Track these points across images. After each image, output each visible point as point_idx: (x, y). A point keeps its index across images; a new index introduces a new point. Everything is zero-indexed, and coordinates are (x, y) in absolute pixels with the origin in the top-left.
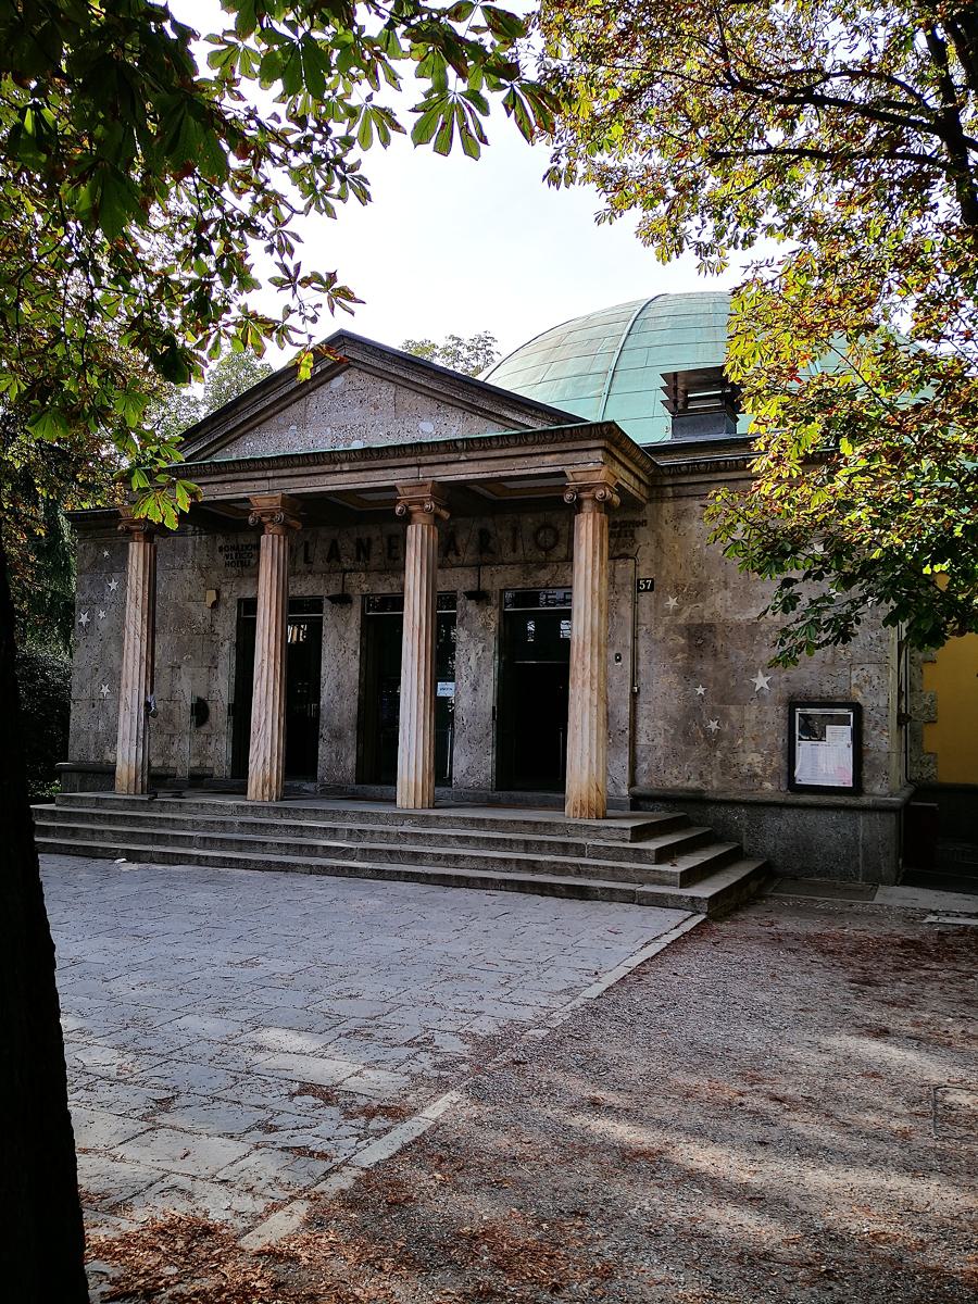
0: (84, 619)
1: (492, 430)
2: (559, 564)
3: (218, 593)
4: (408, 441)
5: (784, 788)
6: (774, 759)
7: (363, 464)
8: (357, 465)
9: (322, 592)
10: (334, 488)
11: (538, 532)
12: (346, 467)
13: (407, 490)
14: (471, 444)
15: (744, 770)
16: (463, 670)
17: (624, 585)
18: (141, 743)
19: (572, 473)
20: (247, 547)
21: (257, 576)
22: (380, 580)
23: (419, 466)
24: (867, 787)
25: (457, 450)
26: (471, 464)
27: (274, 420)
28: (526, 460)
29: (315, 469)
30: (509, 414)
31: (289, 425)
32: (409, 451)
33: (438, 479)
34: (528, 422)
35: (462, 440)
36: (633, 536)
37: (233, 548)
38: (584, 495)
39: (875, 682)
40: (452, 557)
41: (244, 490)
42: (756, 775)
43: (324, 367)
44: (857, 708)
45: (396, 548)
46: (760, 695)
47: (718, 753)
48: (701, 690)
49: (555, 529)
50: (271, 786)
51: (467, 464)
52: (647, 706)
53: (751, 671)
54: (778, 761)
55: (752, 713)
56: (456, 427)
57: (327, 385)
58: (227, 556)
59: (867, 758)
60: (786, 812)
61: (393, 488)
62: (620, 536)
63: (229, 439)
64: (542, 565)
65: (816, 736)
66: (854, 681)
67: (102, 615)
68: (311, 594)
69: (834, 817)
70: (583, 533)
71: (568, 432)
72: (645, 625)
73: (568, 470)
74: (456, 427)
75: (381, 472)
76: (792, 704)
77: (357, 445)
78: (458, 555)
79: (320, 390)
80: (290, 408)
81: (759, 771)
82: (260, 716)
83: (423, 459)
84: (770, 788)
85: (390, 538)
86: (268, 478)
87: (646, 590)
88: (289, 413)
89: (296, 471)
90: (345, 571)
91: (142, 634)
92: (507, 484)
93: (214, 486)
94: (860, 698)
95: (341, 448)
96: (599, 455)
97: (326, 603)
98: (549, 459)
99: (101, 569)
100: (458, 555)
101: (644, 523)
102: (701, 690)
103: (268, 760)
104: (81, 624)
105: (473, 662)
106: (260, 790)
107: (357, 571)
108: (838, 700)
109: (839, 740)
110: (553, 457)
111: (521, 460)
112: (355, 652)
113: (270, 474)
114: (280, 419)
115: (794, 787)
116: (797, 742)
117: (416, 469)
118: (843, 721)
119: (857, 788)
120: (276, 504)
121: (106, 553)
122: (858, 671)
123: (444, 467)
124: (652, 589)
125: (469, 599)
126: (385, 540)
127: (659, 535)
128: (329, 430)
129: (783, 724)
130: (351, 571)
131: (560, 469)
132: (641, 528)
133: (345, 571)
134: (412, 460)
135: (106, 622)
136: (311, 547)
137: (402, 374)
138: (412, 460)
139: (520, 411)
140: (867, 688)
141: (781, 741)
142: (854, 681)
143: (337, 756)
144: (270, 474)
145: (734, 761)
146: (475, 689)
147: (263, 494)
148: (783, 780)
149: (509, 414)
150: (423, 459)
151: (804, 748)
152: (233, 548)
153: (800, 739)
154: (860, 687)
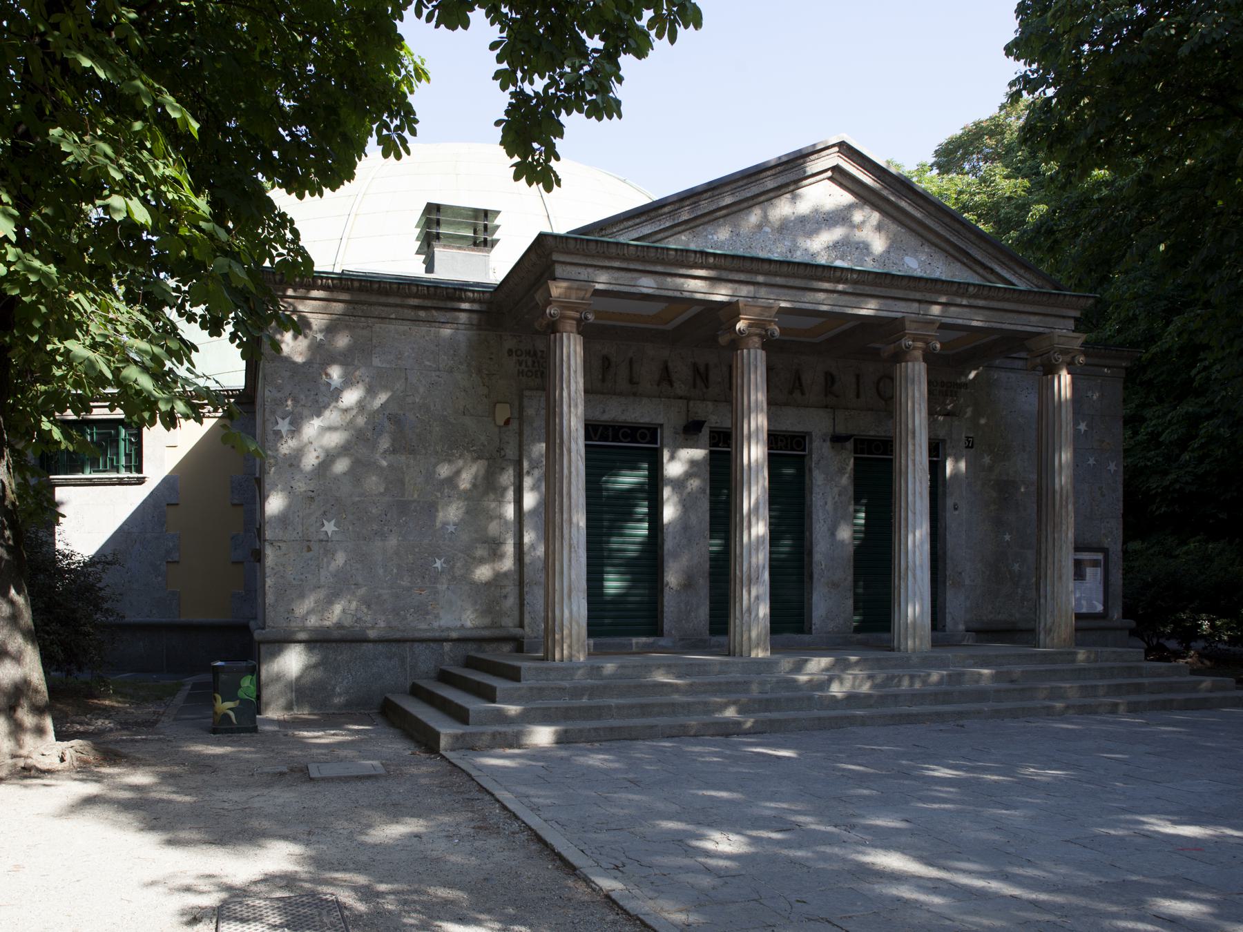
28: (1015, 316)
34: (1014, 279)
37: (528, 353)
47: (1020, 591)
48: (1007, 537)
58: (520, 364)
78: (803, 394)
89: (791, 282)
100: (803, 394)
102: (1007, 537)
105: (829, 507)
111: (1011, 315)
113: (760, 279)
117: (916, 305)
138: (918, 296)
152: (528, 353)
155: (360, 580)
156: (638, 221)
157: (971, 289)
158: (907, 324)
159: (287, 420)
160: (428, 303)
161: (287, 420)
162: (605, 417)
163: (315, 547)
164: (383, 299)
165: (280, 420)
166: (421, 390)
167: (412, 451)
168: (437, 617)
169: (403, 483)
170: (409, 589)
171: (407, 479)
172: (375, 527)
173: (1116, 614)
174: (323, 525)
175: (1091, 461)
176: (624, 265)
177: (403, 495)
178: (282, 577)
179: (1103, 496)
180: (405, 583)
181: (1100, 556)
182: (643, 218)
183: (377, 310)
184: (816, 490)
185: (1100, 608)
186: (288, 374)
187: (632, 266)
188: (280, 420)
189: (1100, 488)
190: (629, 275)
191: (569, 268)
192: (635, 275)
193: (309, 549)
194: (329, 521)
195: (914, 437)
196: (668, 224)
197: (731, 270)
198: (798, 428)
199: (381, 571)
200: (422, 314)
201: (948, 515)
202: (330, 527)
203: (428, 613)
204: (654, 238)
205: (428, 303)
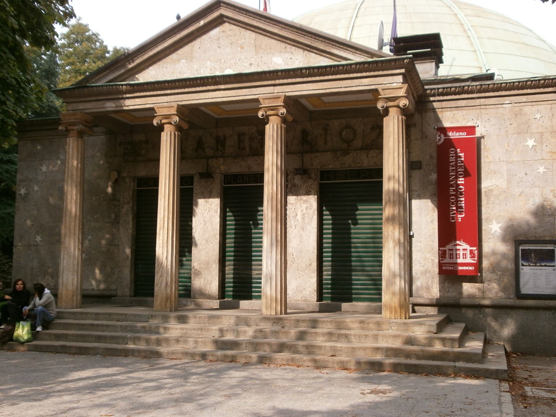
0: (23, 191)
2: (358, 152)
3: (119, 173)
4: (266, 69)
5: (512, 296)
6: (506, 277)
9: (191, 172)
10: (214, 100)
11: (342, 131)
13: (267, 101)
16: (293, 222)
18: (75, 274)
19: (383, 89)
21: (158, 160)
23: (274, 85)
31: (179, 60)
33: (287, 94)
41: (150, 102)
50: (171, 302)
52: (419, 244)
56: (299, 59)
61: (257, 100)
64: (346, 152)
65: (532, 262)
67: (36, 188)
70: (391, 129)
72: (416, 191)
82: (163, 254)
85: (239, 135)
88: (180, 52)
89: (187, 90)
90: (208, 158)
91: (76, 199)
92: (323, 98)
96: (400, 79)
97: (196, 179)
103: (169, 283)
105: (299, 217)
106: (163, 304)
107: (216, 158)
108: (547, 239)
112: (216, 211)
114: (174, 56)
115: (520, 296)
116: (521, 267)
117: (272, 87)
120: (173, 111)
121: (39, 147)
125: (296, 174)
128: (208, 62)
130: (212, 157)
131: (373, 87)
133: (208, 158)
143: (180, 279)
147: (165, 105)
148: (512, 290)
150: (278, 82)
153: (523, 265)
156: (104, 73)
157: (304, 71)
158: (261, 101)
159: (24, 189)
165: (22, 189)
176: (96, 98)
182: (107, 71)
187: (100, 98)
190: (101, 102)
192: (104, 102)
194: (38, 236)
202: (39, 239)
204: (119, 80)
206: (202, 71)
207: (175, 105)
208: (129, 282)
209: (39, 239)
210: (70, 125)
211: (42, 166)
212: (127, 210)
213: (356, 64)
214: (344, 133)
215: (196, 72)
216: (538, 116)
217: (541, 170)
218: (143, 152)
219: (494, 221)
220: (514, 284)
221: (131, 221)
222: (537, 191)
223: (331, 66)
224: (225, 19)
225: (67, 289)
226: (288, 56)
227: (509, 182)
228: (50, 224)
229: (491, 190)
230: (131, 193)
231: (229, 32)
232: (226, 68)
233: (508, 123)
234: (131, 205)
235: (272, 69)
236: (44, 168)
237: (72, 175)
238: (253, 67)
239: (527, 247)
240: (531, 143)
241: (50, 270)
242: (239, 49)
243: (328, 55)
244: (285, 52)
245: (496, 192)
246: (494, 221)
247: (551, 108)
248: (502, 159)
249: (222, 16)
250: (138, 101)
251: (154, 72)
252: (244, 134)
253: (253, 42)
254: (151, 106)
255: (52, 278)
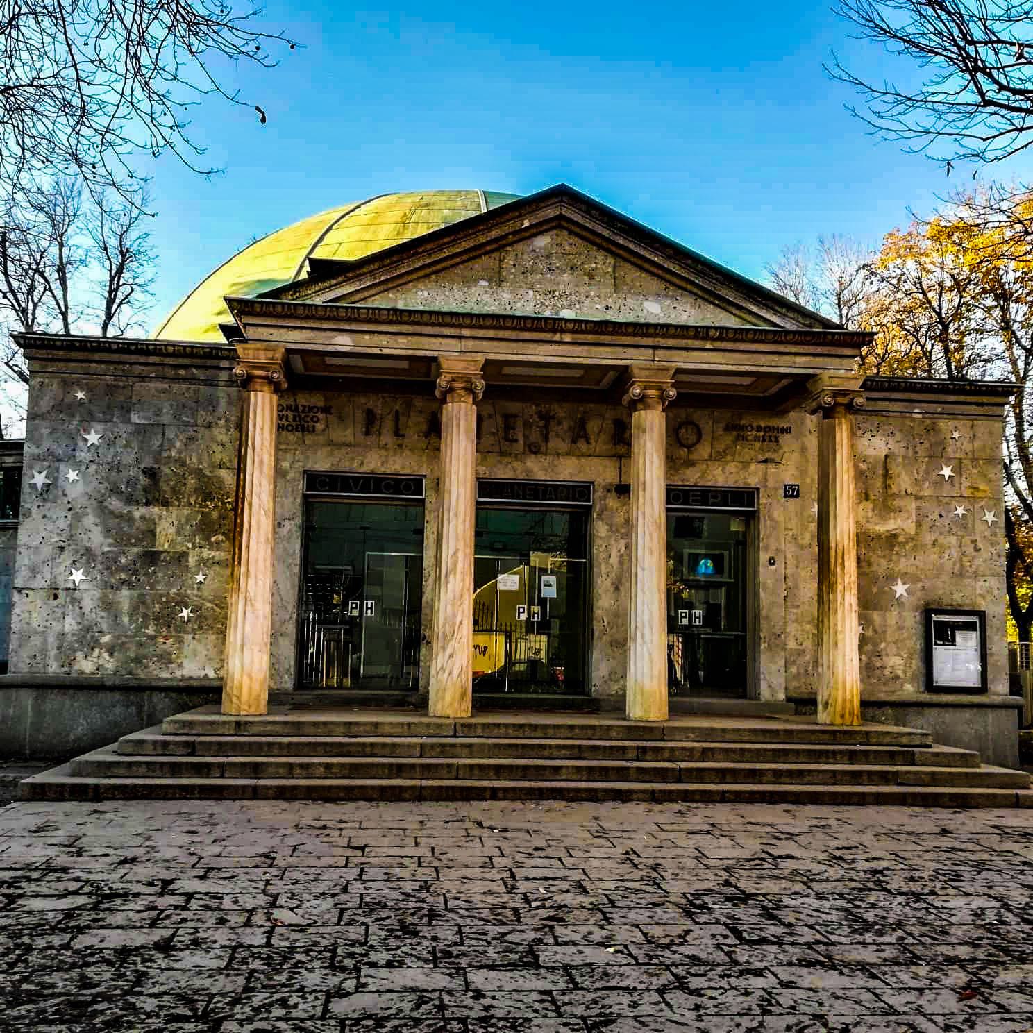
1: (731, 322)
7: (590, 338)
8: (581, 337)
12: (568, 338)
14: (724, 334)
15: (887, 672)
16: (603, 567)
17: (776, 489)
20: (311, 409)
22: (500, 462)
23: (655, 348)
24: (992, 687)
25: (706, 338)
26: (715, 354)
27: (458, 270)
28: (775, 358)
29: (527, 335)
30: (755, 309)
32: (651, 331)
35: (716, 328)
36: (777, 441)
38: (840, 400)
39: (996, 592)
40: (582, 445)
42: (897, 677)
43: (534, 222)
44: (982, 615)
45: (514, 429)
46: (899, 602)
49: (697, 427)
51: (711, 354)
53: (891, 578)
54: (916, 664)
55: (892, 617)
56: (687, 313)
57: (529, 242)
59: (990, 660)
60: (927, 711)
62: (764, 441)
63: (398, 283)
66: (978, 591)
68: (408, 471)
69: (968, 714)
71: (830, 337)
73: (826, 374)
74: (687, 313)
75: (608, 349)
76: (928, 611)
77: (566, 314)
79: (519, 247)
80: (479, 260)
81: (900, 673)
83: (662, 342)
84: (910, 691)
86: (460, 337)
87: (792, 496)
89: (501, 334)
93: (382, 337)
94: (982, 605)
95: (547, 314)
98: (800, 360)
99: (73, 415)
100: (588, 443)
101: (787, 430)
104: (34, 486)
108: (966, 608)
109: (967, 642)
110: (804, 359)
117: (651, 351)
118: (969, 627)
119: (983, 689)
120: (474, 369)
122: (982, 583)
123: (683, 353)
124: (797, 496)
126: (500, 420)
127: (803, 443)
128: (531, 293)
129: (919, 629)
132: (787, 436)
134: (649, 341)
135: (80, 488)
136: (402, 419)
137: (631, 246)
139: (768, 308)
140: (989, 598)
141: (918, 645)
142: (978, 591)
144: (466, 332)
145: (878, 664)
146: (617, 589)
147: (459, 357)
148: (922, 679)
149: (755, 309)
151: (941, 653)
154: (983, 597)
155: (104, 627)
158: (636, 371)
159: (44, 474)
160: (186, 361)
161: (44, 474)
162: (364, 469)
163: (61, 594)
164: (142, 359)
165: (36, 474)
166: (178, 444)
167: (166, 503)
168: (180, 666)
169: (154, 535)
170: (153, 638)
171: (158, 530)
172: (123, 576)
173: (1000, 687)
174: (71, 574)
175: (960, 511)
177: (153, 546)
178: (28, 624)
179: (977, 550)
180: (150, 631)
181: (975, 619)
183: (137, 369)
184: (597, 542)
185: (973, 681)
186: (48, 430)
187: (325, 326)
188: (36, 474)
189: (974, 542)
191: (260, 330)
193: (56, 597)
195: (644, 490)
196: (368, 284)
197: (433, 325)
198: (580, 478)
199: (126, 619)
200: (182, 372)
201: (761, 570)
202: (78, 576)
203: (171, 662)
205: (186, 361)
206: (519, 305)
207: (481, 358)
208: (292, 663)
209: (78, 576)
210: (254, 368)
211: (87, 431)
212: (290, 530)
213: (794, 333)
214: (683, 431)
215: (508, 307)
216: (956, 435)
217: (960, 511)
218: (319, 426)
219: (900, 582)
220: (924, 671)
221: (298, 551)
222: (953, 540)
223: (736, 330)
224: (565, 224)
225: (251, 678)
226: (668, 302)
227: (919, 525)
228: (106, 549)
229: (895, 536)
230: (299, 501)
231: (568, 248)
232: (563, 307)
233: (918, 440)
234: (298, 520)
235: (643, 321)
236: (93, 438)
237: (261, 462)
238: (610, 312)
239: (935, 618)
240: (947, 472)
241: (106, 639)
242: (586, 278)
243: (736, 312)
244: (666, 296)
245: (901, 539)
246: (900, 582)
247: (972, 426)
248: (909, 491)
249: (561, 217)
250: (402, 341)
251: (426, 294)
252: (515, 416)
253: (610, 270)
254: (436, 354)
255: (111, 655)
